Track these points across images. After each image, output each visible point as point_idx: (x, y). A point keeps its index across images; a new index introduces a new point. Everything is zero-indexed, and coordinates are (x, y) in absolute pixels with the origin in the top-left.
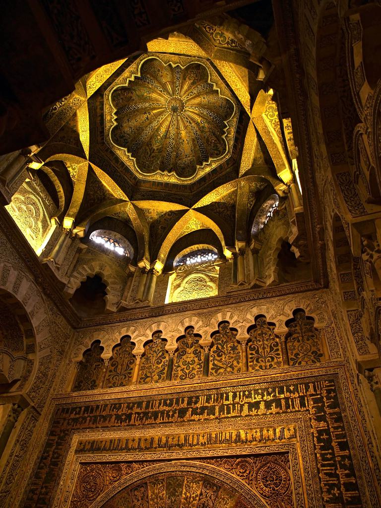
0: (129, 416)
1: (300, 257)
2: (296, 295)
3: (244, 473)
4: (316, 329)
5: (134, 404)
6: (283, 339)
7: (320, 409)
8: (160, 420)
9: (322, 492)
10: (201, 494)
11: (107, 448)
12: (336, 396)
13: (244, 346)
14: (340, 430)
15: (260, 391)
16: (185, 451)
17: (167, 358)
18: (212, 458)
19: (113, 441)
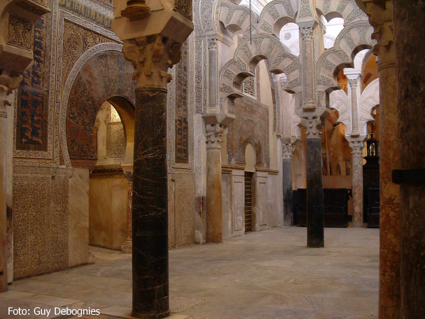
14: (185, 59)
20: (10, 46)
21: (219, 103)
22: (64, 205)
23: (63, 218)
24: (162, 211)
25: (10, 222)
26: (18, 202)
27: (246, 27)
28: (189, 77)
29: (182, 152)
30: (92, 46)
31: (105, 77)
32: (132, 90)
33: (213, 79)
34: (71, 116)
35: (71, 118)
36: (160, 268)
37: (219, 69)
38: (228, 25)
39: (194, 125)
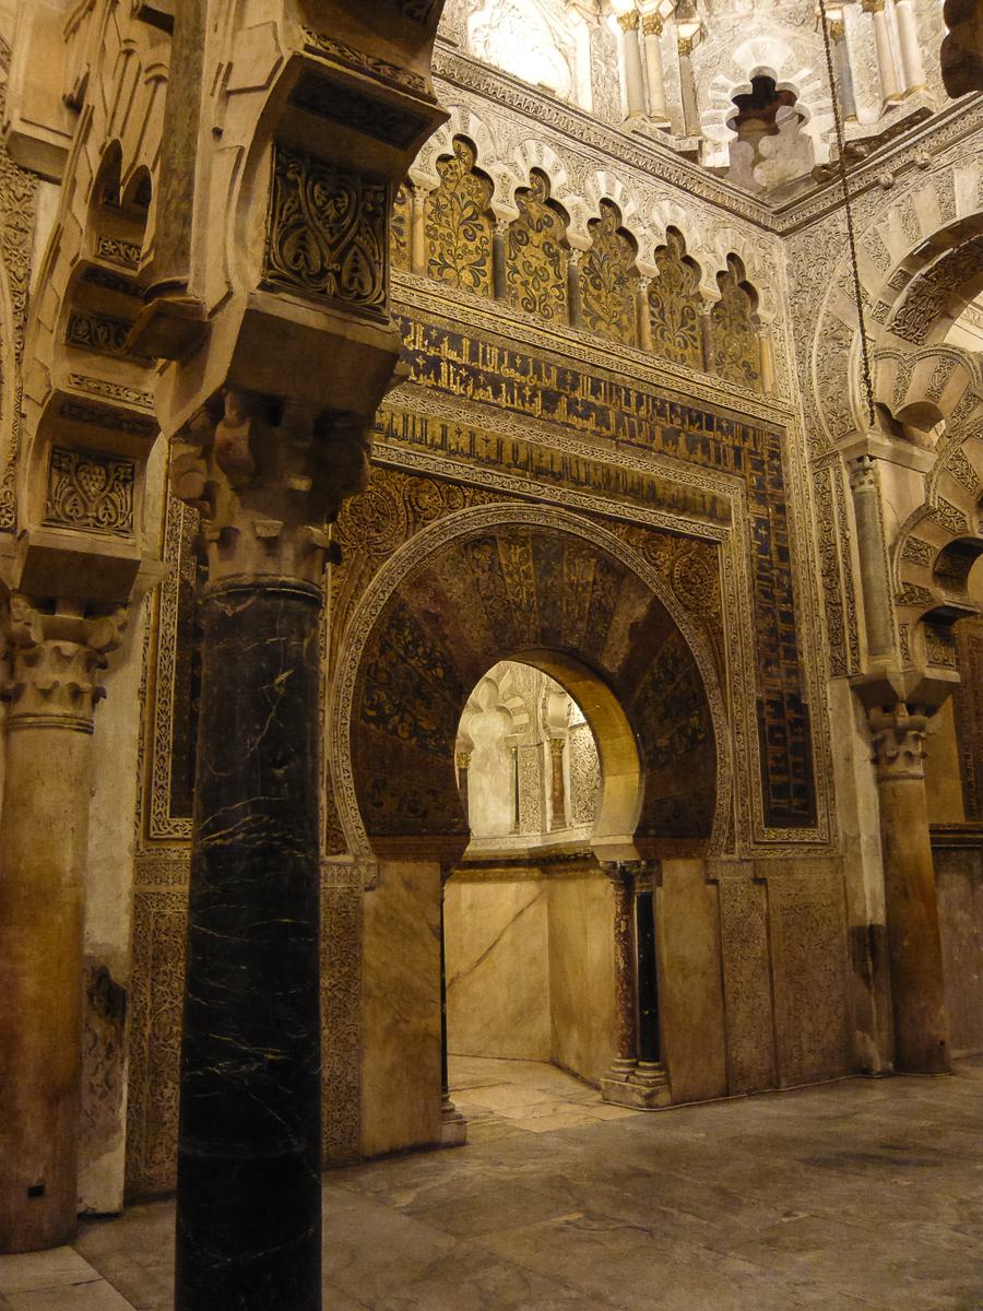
0: (433, 365)
1: (824, 167)
2: (734, 219)
3: (656, 559)
4: (757, 319)
5: (442, 334)
6: (707, 311)
7: (760, 485)
8: (507, 401)
9: (756, 617)
10: (595, 583)
11: (400, 433)
12: (780, 466)
13: (644, 292)
14: (782, 527)
15: (679, 410)
16: (565, 490)
17: (487, 232)
18: (610, 519)
19: (410, 419)
20: (55, 531)
21: (898, 640)
22: (347, 969)
23: (340, 1009)
24: (259, 1058)
25: (116, 1029)
26: (170, 967)
27: (954, 403)
28: (802, 576)
29: (792, 794)
30: (439, 518)
31: (489, 598)
32: (593, 627)
33: (871, 571)
34: (372, 713)
35: (368, 720)
36: (243, 1300)
37: (889, 541)
38: (899, 409)
39: (830, 713)
